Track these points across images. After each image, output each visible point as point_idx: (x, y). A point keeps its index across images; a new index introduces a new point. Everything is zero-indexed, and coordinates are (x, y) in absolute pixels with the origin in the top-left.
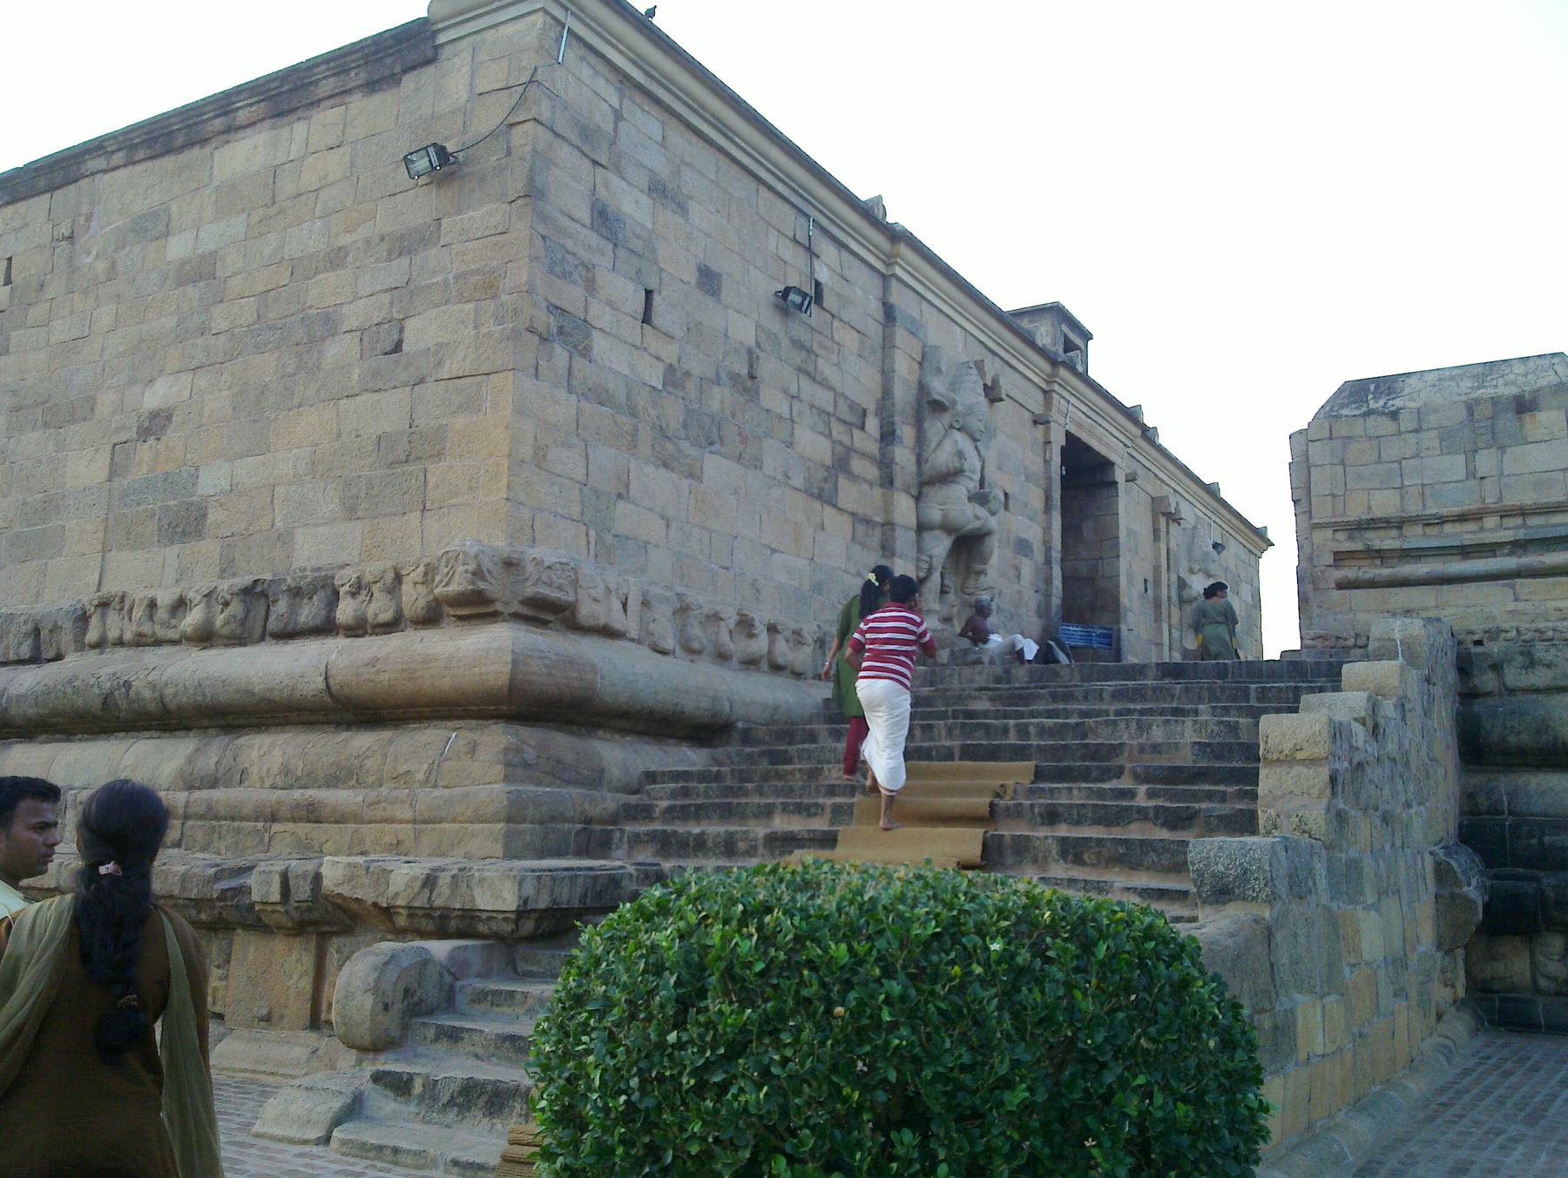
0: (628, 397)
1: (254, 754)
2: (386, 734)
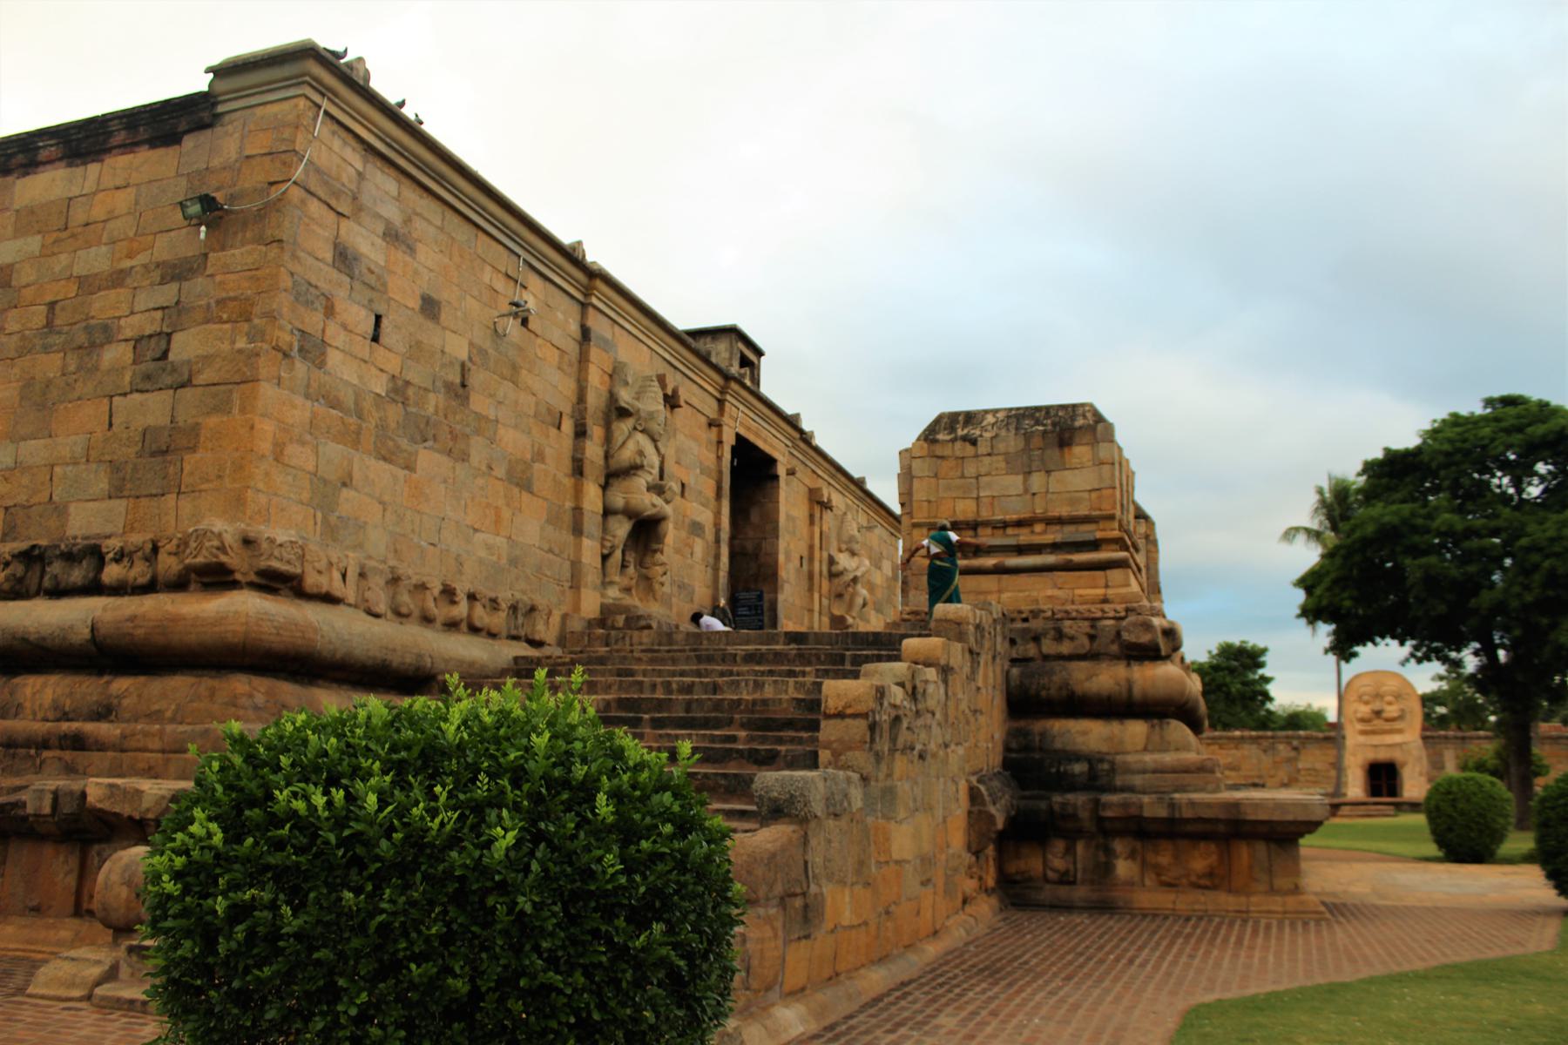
0: (356, 403)
1: (28, 691)
2: (142, 679)
